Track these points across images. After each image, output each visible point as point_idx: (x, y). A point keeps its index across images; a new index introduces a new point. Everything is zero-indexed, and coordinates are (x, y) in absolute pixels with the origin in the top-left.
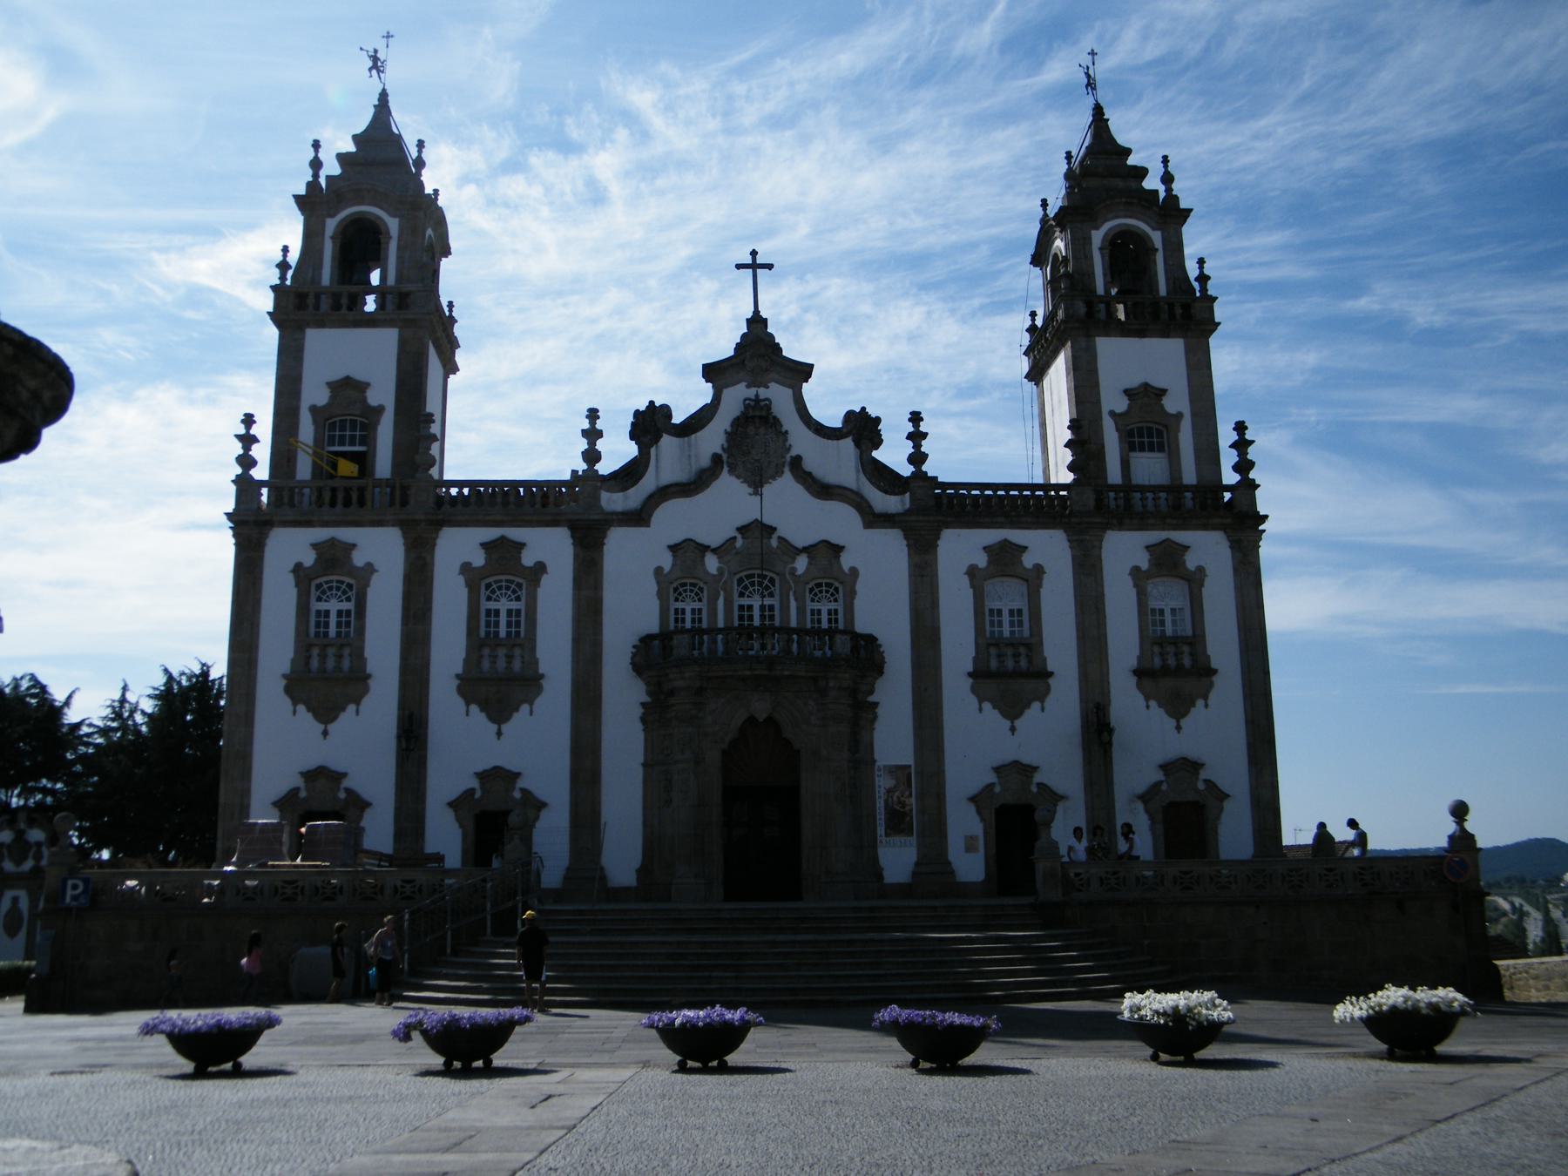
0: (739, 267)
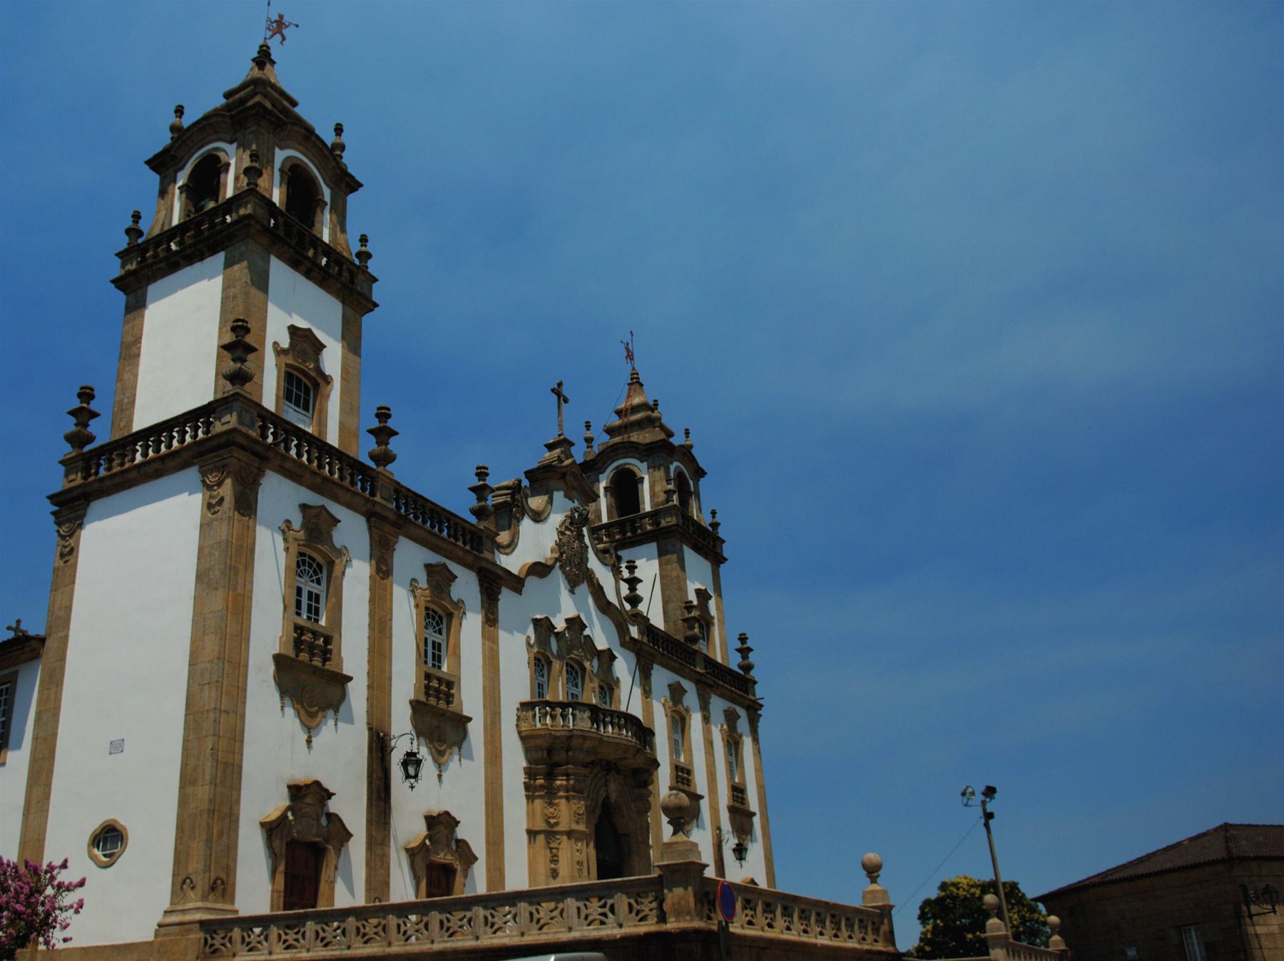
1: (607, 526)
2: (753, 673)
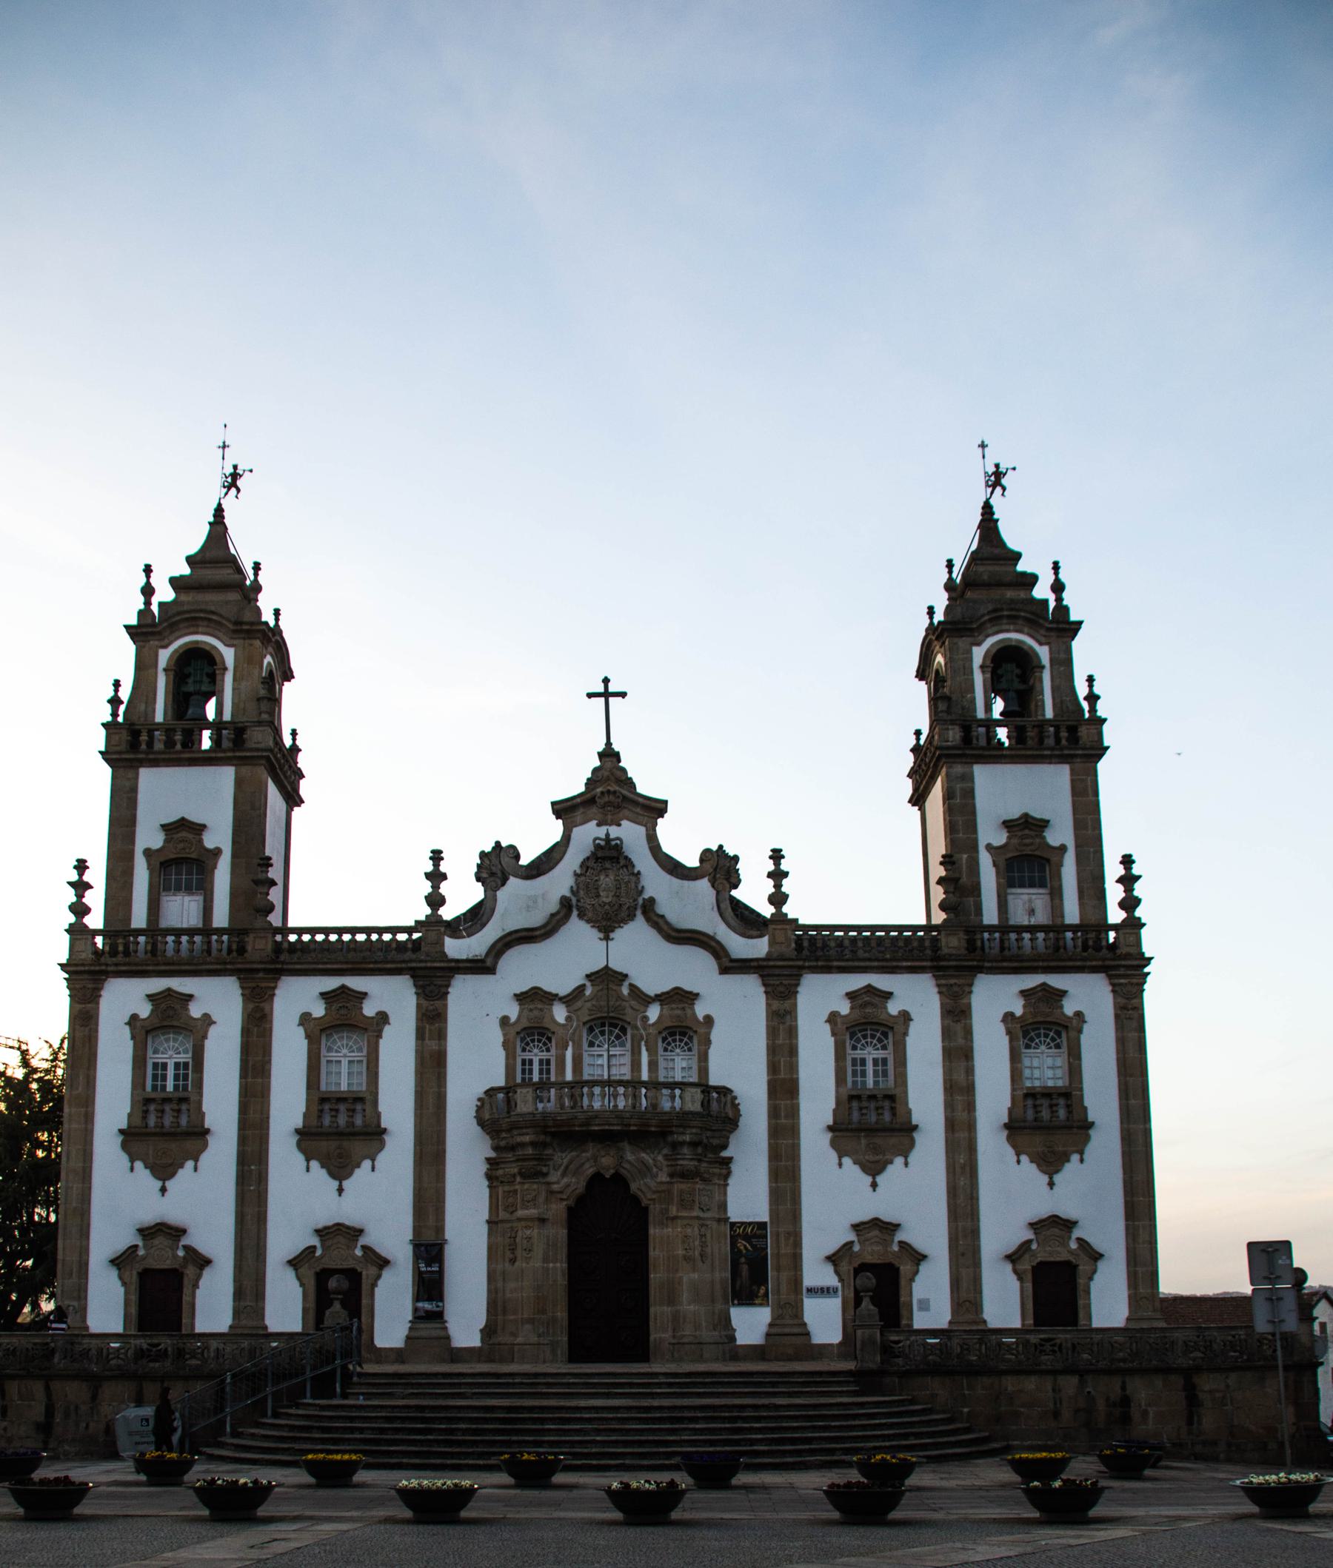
0: (590, 695)
2: (1138, 913)
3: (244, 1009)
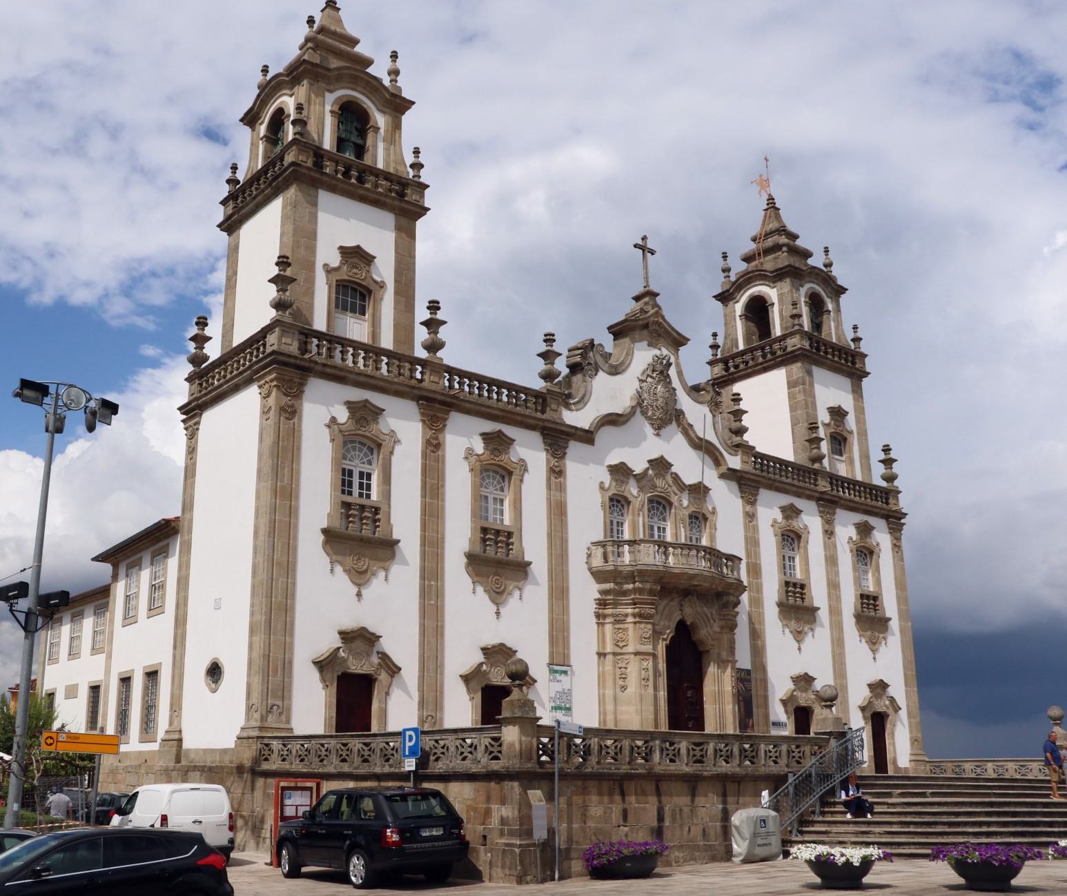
1: (743, 353)
2: (896, 483)
3: (424, 433)
